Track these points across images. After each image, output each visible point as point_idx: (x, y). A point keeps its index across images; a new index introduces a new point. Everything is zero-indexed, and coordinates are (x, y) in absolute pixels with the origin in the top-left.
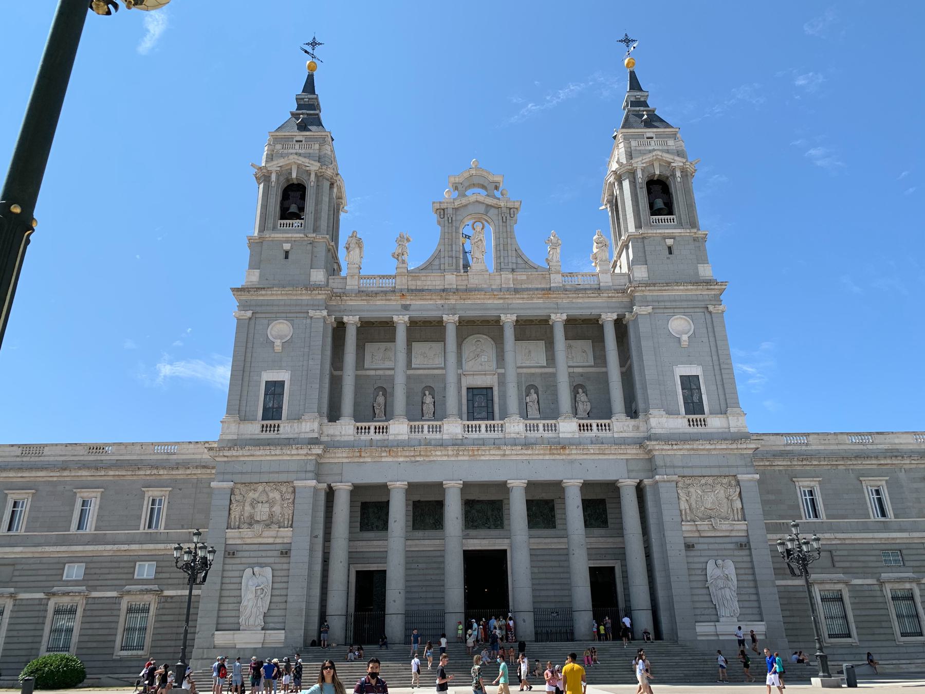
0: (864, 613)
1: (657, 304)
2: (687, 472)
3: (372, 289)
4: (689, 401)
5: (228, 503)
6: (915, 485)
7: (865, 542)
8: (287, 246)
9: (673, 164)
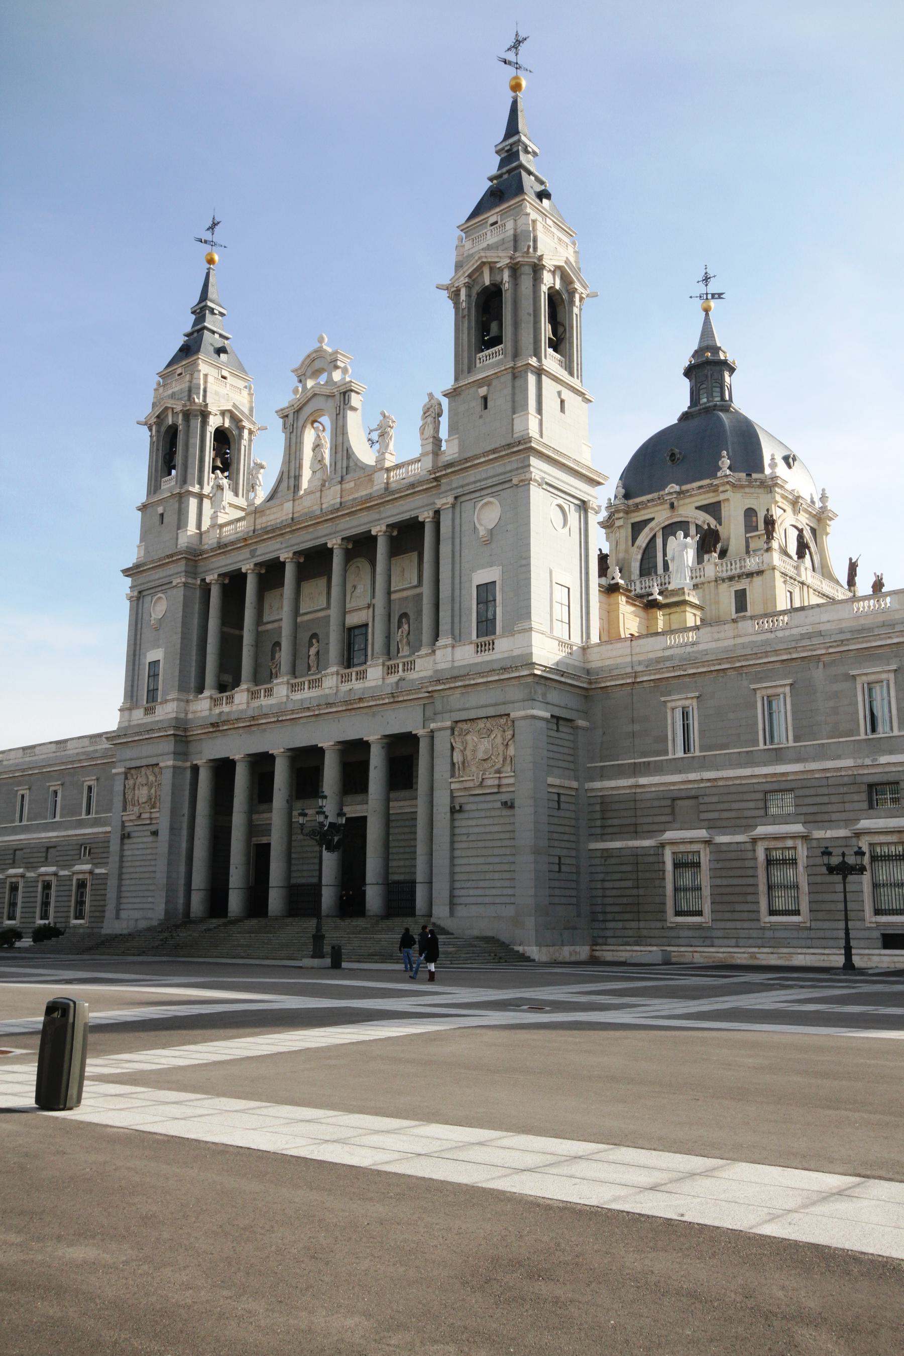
0: (725, 882)
1: (461, 490)
2: (464, 715)
3: (228, 538)
4: (484, 619)
5: (122, 788)
6: (835, 687)
7: (743, 782)
8: (160, 510)
9: (498, 265)
